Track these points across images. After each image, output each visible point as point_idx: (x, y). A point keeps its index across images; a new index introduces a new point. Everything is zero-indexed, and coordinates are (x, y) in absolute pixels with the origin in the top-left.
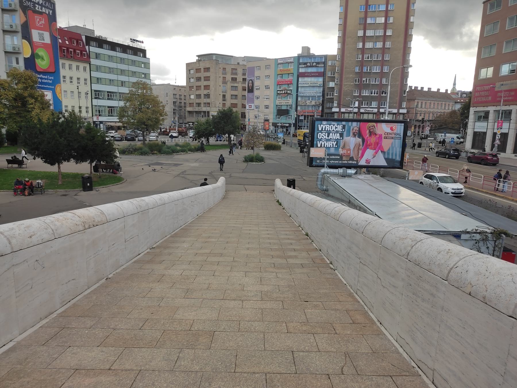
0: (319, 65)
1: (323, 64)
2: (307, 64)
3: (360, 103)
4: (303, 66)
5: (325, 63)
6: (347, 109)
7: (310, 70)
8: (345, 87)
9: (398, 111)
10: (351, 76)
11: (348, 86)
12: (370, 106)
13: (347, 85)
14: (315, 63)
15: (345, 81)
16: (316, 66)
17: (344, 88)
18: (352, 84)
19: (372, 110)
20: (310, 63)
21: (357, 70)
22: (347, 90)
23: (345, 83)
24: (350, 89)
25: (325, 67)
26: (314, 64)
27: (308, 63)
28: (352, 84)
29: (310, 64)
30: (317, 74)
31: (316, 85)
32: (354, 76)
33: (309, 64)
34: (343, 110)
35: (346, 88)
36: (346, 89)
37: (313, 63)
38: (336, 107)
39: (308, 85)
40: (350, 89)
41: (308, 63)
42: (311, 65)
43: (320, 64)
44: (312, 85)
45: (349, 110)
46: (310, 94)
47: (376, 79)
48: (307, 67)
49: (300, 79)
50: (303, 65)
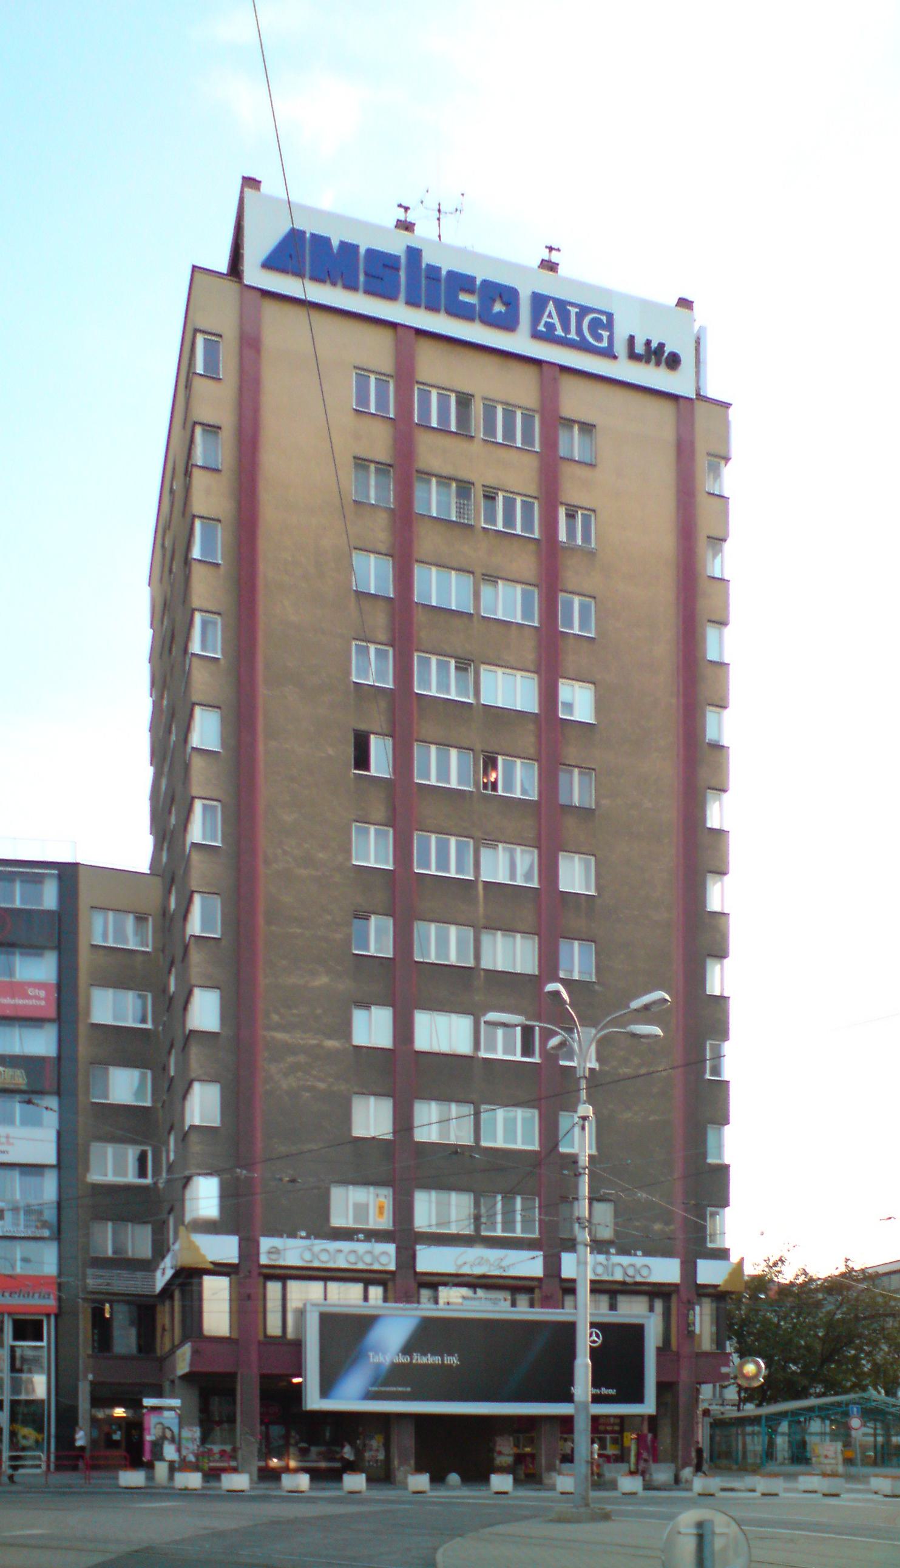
10: (323, 980)
11: (302, 1058)
13: (290, 1049)
15: (275, 1018)
23: (279, 1036)
32: (345, 986)
40: (322, 1086)
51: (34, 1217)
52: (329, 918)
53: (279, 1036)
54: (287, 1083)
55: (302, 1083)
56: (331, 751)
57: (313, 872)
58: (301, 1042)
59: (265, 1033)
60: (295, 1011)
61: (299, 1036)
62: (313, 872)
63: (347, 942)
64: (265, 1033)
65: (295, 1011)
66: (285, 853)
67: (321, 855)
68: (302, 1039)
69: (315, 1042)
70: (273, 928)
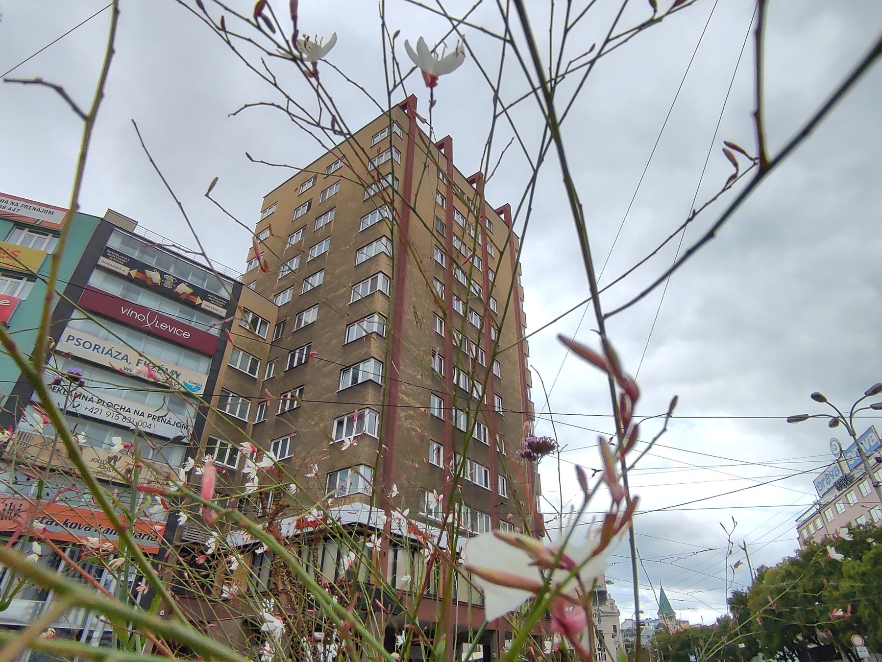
0: (205, 305)
2: (149, 273)
4: (125, 270)
7: (146, 300)
14: (190, 285)
16: (186, 302)
20: (162, 274)
22: (409, 430)
26: (182, 288)
27: (152, 269)
29: (162, 278)
30: (186, 335)
33: (156, 277)
35: (406, 419)
37: (180, 282)
41: (152, 269)
42: (168, 285)
43: (209, 301)
50: (125, 264)
53: (405, 398)
54: (407, 424)
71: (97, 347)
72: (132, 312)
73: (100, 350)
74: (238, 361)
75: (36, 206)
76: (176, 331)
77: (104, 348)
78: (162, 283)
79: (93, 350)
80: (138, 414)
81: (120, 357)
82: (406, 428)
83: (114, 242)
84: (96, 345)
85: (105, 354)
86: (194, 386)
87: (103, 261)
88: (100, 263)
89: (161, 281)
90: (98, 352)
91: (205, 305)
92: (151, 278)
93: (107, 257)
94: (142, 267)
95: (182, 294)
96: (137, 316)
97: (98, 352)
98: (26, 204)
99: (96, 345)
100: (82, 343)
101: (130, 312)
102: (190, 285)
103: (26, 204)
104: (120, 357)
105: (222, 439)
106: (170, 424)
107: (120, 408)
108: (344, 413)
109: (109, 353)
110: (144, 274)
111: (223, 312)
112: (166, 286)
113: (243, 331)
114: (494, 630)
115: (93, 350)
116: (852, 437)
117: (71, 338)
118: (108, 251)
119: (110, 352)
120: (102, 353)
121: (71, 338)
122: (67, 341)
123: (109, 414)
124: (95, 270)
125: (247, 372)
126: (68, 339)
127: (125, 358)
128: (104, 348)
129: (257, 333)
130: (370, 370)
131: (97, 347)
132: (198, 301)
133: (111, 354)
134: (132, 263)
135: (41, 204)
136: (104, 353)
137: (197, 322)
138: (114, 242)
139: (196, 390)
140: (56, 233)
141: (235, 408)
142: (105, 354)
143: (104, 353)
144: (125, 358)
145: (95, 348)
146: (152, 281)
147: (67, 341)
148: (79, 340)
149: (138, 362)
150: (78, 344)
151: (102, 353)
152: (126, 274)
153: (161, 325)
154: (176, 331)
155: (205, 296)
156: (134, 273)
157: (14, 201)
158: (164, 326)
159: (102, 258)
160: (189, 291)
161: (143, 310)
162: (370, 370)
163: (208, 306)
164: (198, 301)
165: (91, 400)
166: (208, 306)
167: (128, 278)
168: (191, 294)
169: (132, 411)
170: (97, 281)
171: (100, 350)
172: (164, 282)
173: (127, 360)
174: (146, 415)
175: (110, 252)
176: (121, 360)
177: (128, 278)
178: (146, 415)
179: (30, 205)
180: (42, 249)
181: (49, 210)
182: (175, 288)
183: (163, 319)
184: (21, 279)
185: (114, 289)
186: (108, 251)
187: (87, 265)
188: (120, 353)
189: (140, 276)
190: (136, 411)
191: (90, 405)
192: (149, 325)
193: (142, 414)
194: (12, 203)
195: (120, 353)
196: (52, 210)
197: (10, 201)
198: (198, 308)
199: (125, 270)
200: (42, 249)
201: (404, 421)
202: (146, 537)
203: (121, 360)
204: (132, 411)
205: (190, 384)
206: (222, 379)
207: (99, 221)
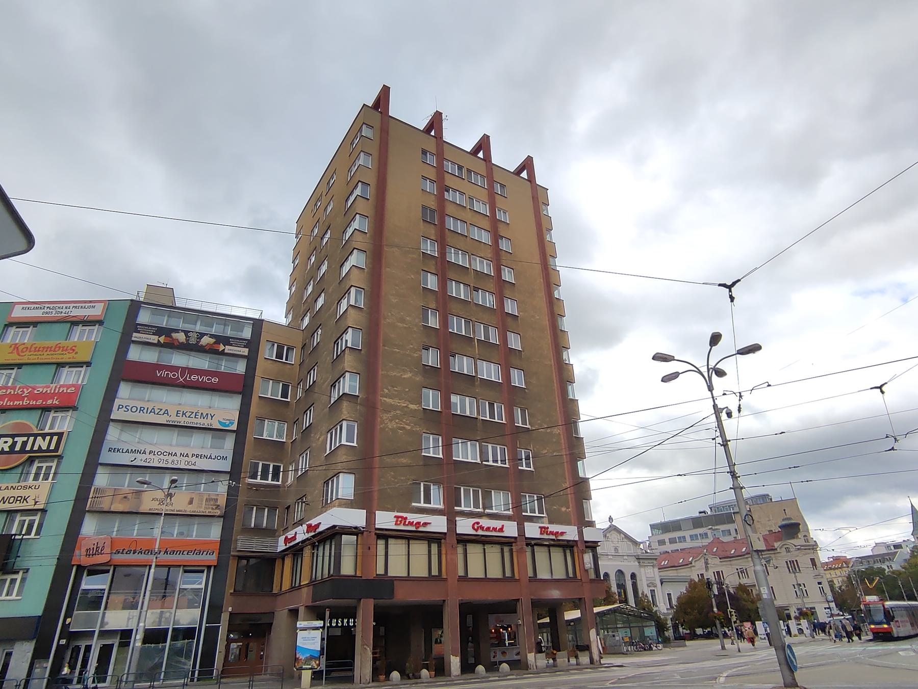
0: (228, 349)
1: (245, 347)
2: (174, 335)
3: (452, 499)
4: (154, 339)
5: (253, 344)
6: (405, 515)
7: (179, 359)
8: (385, 416)
9: (581, 533)
10: (408, 375)
12: (487, 511)
13: (395, 408)
14: (212, 336)
15: (386, 391)
17: (382, 422)
18: (412, 406)
19: (497, 524)
20: (186, 333)
21: (432, 358)
22: (393, 430)
23: (388, 400)
24: (408, 427)
25: (252, 360)
26: (206, 340)
27: (177, 331)
28: (412, 406)
29: (187, 336)
30: (215, 380)
31: (205, 423)
32: (418, 378)
33: (181, 337)
34: (385, 520)
35: (391, 421)
36: (393, 423)
37: (202, 335)
38: (350, 504)
39: (162, 419)
40: (408, 427)
41: (177, 331)
42: (193, 341)
43: (231, 345)
44: (183, 421)
45: (411, 524)
46: (171, 458)
47: (491, 405)
48: (172, 346)
49: (125, 390)
51: (212, 503)
52: (412, 346)
53: (388, 400)
55: (399, 425)
56: (413, 277)
57: (405, 326)
58: (399, 404)
59: (381, 398)
60: (395, 389)
61: (397, 401)
62: (405, 326)
63: (420, 358)
64: (381, 398)
65: (395, 389)
66: (392, 314)
67: (408, 318)
68: (399, 403)
69: (405, 405)
70: (386, 348)
71: (142, 409)
72: (166, 373)
73: (145, 411)
74: (266, 389)
75: (84, 305)
76: (205, 379)
77: (148, 408)
78: (187, 340)
79: (140, 412)
80: (183, 456)
81: (162, 413)
82: (391, 429)
83: (144, 317)
84: (141, 407)
85: (150, 413)
86: (228, 422)
87: (136, 336)
88: (133, 339)
89: (186, 339)
90: (143, 413)
91: (228, 349)
92: (177, 339)
93: (138, 332)
94: (167, 332)
95: (206, 346)
96: (171, 375)
97: (143, 413)
98: (75, 305)
99: (141, 407)
100: (129, 408)
101: (164, 373)
102: (212, 336)
103: (75, 305)
104: (162, 413)
105: (262, 461)
106: (211, 458)
107: (168, 454)
108: (332, 427)
109: (153, 411)
110: (171, 337)
111: (245, 351)
112: (191, 343)
113: (270, 362)
114: (519, 599)
115: (140, 412)
116: (710, 392)
117: (121, 407)
118: (138, 327)
119: (153, 411)
120: (147, 413)
121: (121, 407)
122: (118, 410)
123: (160, 461)
124: (132, 344)
125: (279, 398)
126: (119, 408)
127: (166, 412)
128: (148, 408)
129: (284, 360)
130: (349, 385)
131: (142, 409)
132: (222, 347)
133: (154, 412)
134: (159, 331)
135: (85, 302)
136: (149, 412)
137: (224, 366)
138: (144, 317)
139: (230, 425)
140: (100, 323)
141: (272, 431)
142: (150, 413)
143: (149, 412)
144: (166, 412)
145: (140, 410)
146: (178, 341)
147: (118, 410)
148: (127, 407)
149: (177, 413)
150: (127, 410)
151: (147, 413)
152: (156, 342)
153: (192, 377)
154: (205, 379)
155: (227, 341)
156: (162, 339)
157: (67, 305)
158: (194, 378)
159: (135, 334)
160: (212, 341)
161: (174, 369)
162: (349, 385)
163: (230, 350)
164: (222, 347)
165: (145, 453)
166: (230, 350)
167: (159, 345)
168: (215, 343)
169: (178, 455)
170: (135, 354)
171: (145, 411)
172: (189, 340)
173: (168, 414)
174: (190, 456)
175: (140, 327)
176: (163, 414)
177: (159, 345)
178: (190, 456)
179: (78, 305)
180: (93, 340)
181: (92, 304)
182: (200, 341)
183: (192, 371)
184: (82, 367)
185: (150, 356)
186: (138, 327)
187: (125, 343)
188: (161, 410)
189: (169, 340)
190: (181, 454)
191: (144, 457)
192: (181, 380)
193: (187, 455)
194: (66, 308)
195: (161, 410)
196: (94, 304)
197: (64, 305)
198: (223, 353)
199: (154, 339)
200: (93, 340)
201: (387, 422)
202: (205, 553)
203: (163, 414)
204: (178, 455)
205: (225, 422)
206: (254, 410)
207: (129, 303)
